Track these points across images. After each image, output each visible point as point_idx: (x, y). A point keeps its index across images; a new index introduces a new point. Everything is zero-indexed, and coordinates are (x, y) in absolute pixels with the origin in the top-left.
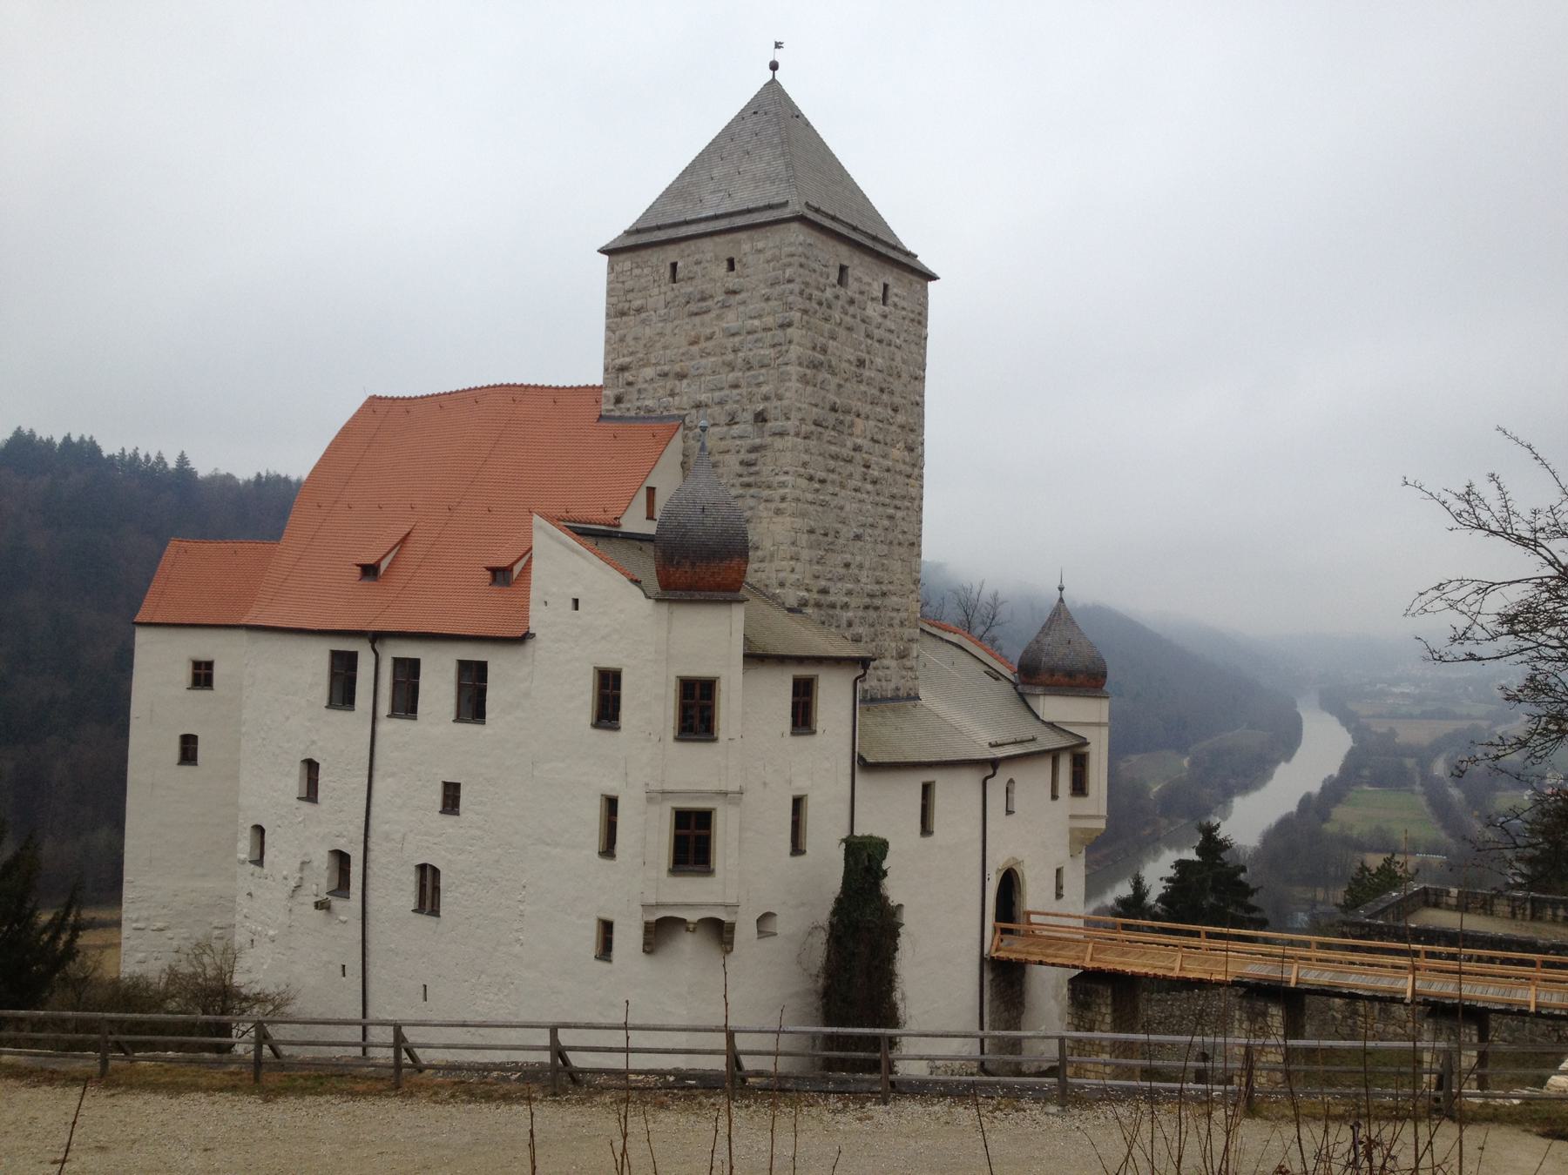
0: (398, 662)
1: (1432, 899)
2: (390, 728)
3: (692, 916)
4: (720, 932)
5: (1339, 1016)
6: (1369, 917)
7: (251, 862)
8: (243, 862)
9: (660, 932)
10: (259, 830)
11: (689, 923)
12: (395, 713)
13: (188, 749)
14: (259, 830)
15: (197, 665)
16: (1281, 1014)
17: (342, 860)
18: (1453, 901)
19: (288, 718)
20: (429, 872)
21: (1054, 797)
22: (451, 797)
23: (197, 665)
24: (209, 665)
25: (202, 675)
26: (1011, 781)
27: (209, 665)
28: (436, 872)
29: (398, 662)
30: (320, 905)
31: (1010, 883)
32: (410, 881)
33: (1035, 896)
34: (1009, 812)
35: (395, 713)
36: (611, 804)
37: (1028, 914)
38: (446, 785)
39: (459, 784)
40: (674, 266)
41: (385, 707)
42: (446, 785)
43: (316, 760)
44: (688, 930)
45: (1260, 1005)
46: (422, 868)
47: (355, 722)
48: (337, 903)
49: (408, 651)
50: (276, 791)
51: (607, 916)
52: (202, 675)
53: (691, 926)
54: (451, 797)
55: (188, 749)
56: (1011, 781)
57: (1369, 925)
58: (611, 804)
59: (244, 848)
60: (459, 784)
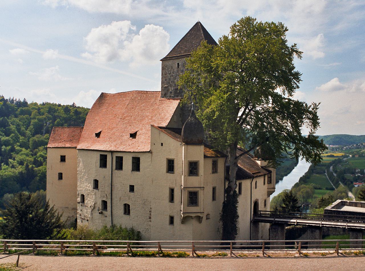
0: (117, 157)
1: (343, 203)
2: (117, 173)
3: (193, 215)
4: (199, 219)
5: (325, 231)
6: (331, 208)
7: (81, 203)
8: (79, 203)
9: (185, 220)
10: (83, 196)
11: (193, 217)
12: (116, 169)
13: (60, 176)
14: (83, 196)
15: (62, 156)
16: (319, 232)
17: (105, 203)
18: (348, 204)
19: (90, 170)
20: (127, 206)
21: (264, 184)
22: (132, 188)
23: (62, 156)
24: (65, 156)
25: (63, 159)
26: (256, 181)
27: (65, 156)
28: (129, 206)
29: (117, 157)
30: (101, 213)
31: (256, 204)
32: (122, 207)
33: (261, 207)
34: (256, 188)
35: (116, 169)
36: (172, 191)
37: (260, 211)
38: (130, 186)
39: (134, 186)
40: (178, 64)
41: (114, 167)
42: (130, 186)
43: (97, 180)
44: (192, 218)
45: (314, 229)
46: (125, 205)
47: (107, 171)
48: (104, 212)
49: (119, 155)
50: (87, 187)
51: (172, 215)
52: (63, 159)
53: (193, 218)
54: (132, 188)
55: (60, 176)
56: (256, 181)
57: (332, 210)
58: (172, 191)
59: (79, 199)
60: (134, 186)
